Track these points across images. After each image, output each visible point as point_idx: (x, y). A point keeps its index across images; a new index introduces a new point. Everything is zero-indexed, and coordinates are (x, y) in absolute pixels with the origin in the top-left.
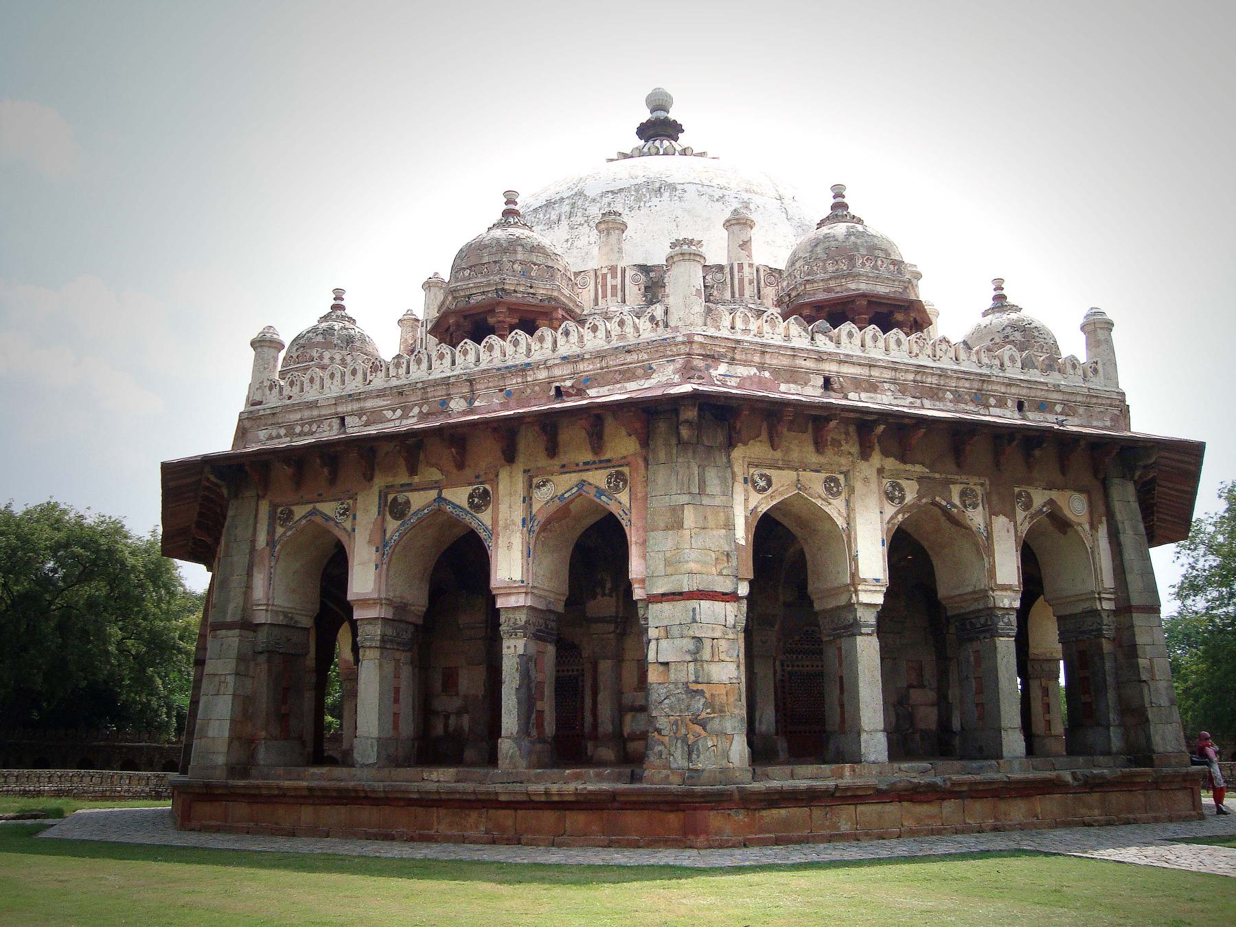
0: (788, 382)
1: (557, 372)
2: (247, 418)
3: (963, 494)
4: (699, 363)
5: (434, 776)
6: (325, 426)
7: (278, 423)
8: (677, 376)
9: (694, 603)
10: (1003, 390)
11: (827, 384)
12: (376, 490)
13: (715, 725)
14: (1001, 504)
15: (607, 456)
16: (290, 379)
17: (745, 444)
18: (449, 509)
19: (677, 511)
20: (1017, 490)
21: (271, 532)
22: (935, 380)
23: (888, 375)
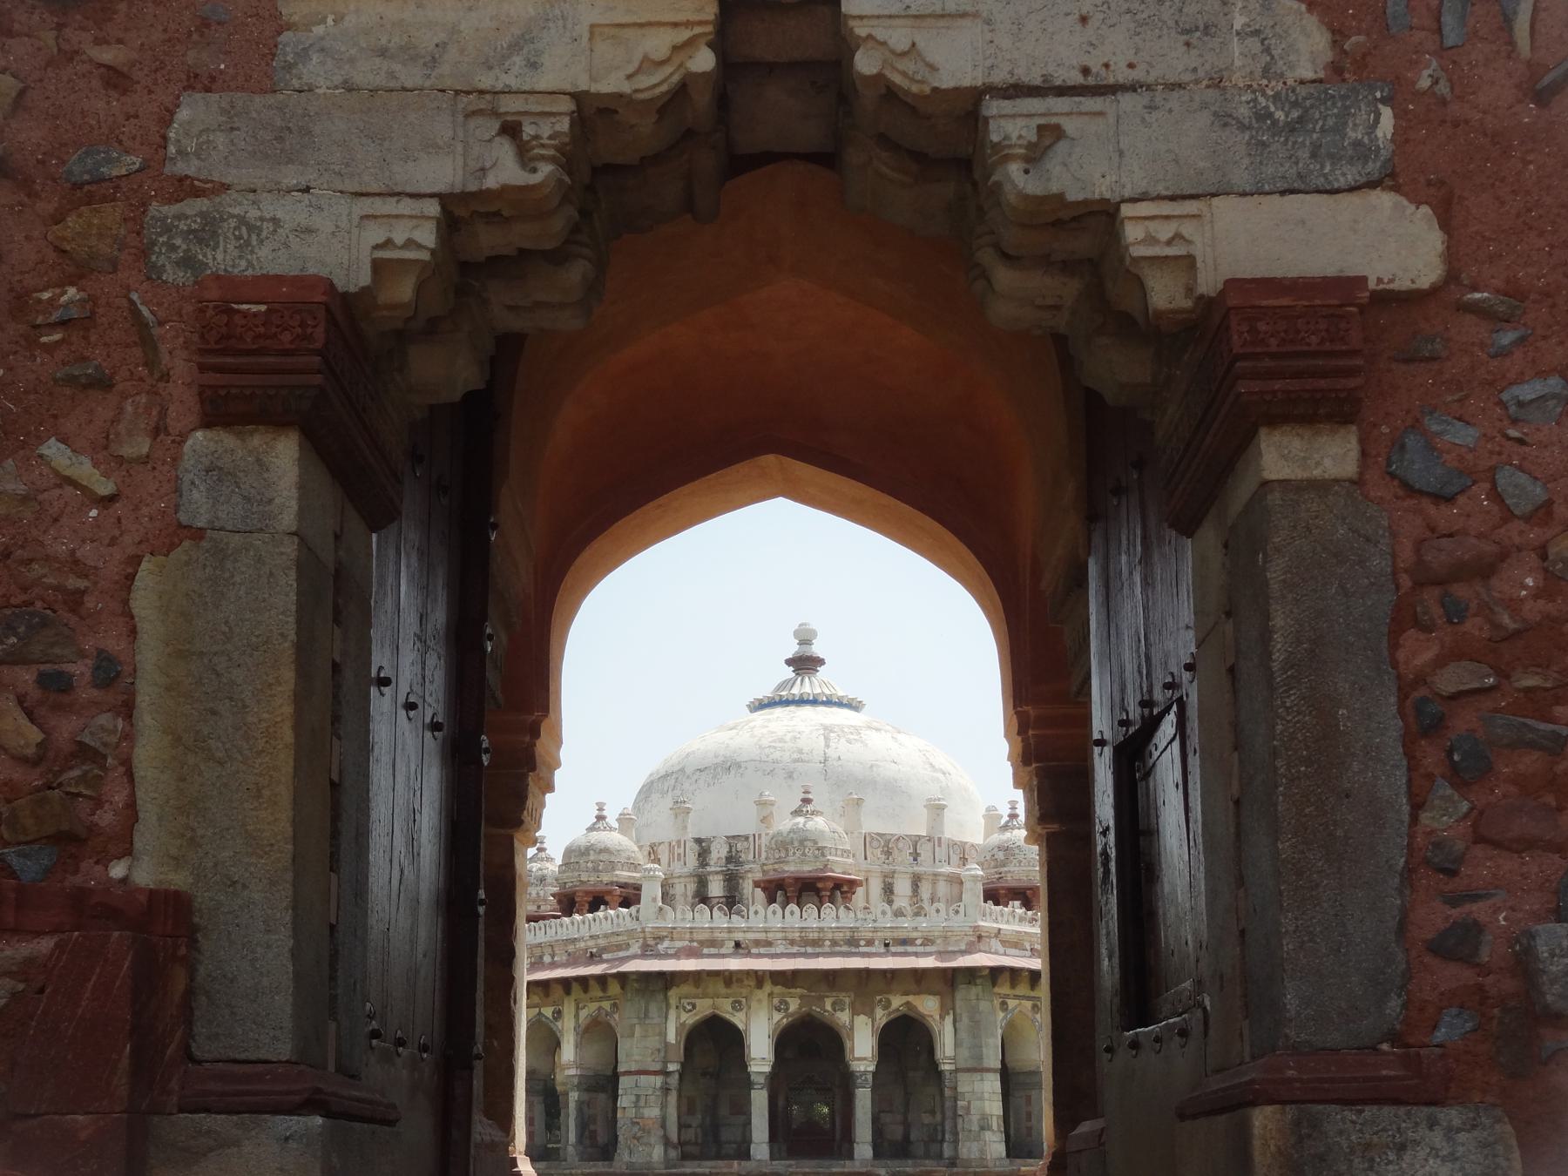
0: (708, 947)
1: (591, 943)
3: (834, 1004)
4: (651, 942)
9: (635, 1077)
10: (871, 934)
11: (738, 945)
13: (645, 1140)
14: (863, 1006)
17: (678, 986)
18: (543, 1019)
19: (632, 1027)
20: (878, 998)
22: (816, 935)
23: (780, 935)
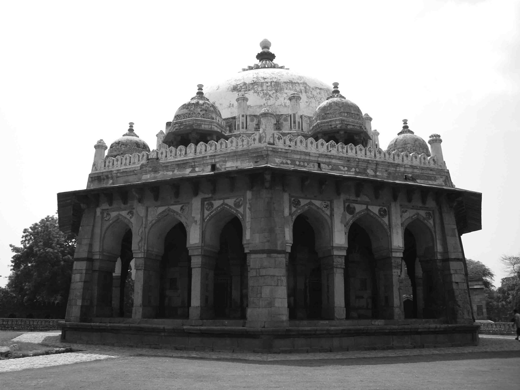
1: (407, 170)
2: (271, 151)
5: (377, 323)
6: (311, 165)
7: (287, 157)
8: (444, 183)
12: (342, 200)
15: (427, 206)
16: (289, 138)
21: (290, 209)
